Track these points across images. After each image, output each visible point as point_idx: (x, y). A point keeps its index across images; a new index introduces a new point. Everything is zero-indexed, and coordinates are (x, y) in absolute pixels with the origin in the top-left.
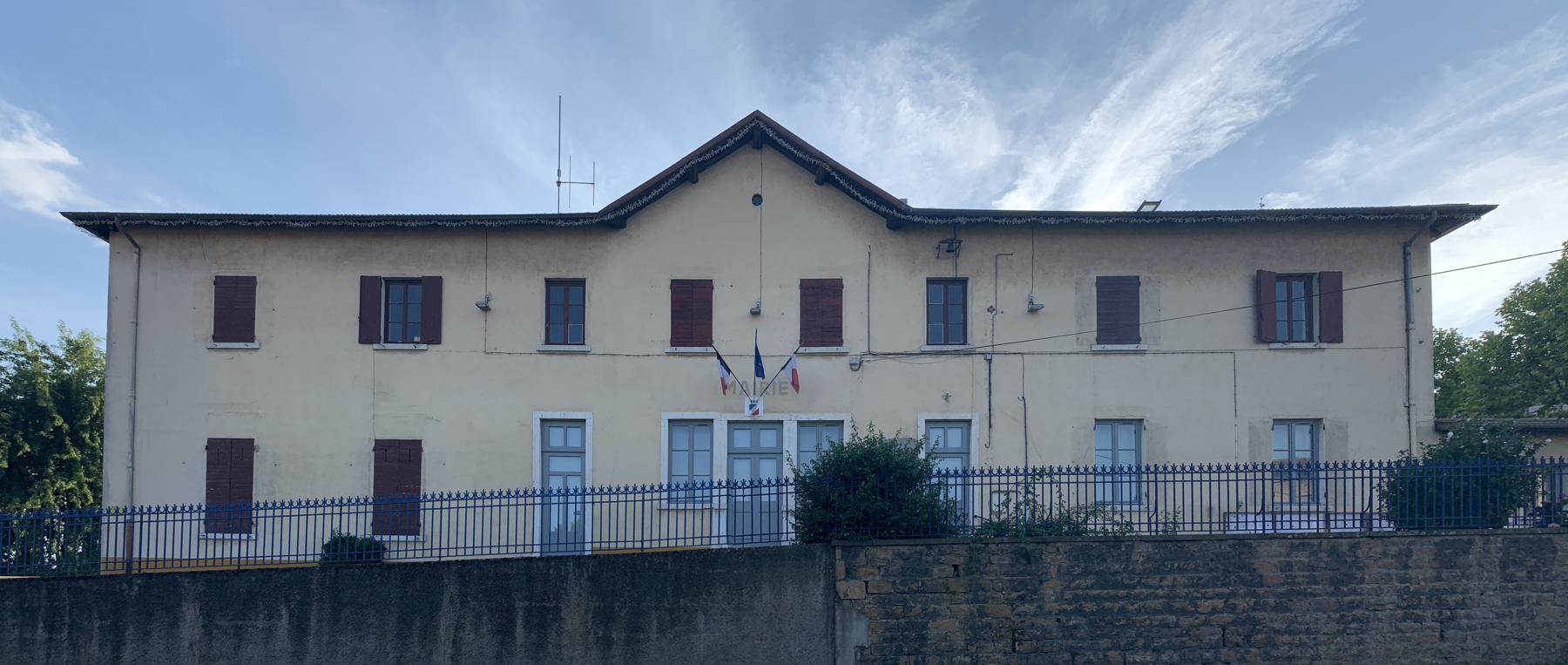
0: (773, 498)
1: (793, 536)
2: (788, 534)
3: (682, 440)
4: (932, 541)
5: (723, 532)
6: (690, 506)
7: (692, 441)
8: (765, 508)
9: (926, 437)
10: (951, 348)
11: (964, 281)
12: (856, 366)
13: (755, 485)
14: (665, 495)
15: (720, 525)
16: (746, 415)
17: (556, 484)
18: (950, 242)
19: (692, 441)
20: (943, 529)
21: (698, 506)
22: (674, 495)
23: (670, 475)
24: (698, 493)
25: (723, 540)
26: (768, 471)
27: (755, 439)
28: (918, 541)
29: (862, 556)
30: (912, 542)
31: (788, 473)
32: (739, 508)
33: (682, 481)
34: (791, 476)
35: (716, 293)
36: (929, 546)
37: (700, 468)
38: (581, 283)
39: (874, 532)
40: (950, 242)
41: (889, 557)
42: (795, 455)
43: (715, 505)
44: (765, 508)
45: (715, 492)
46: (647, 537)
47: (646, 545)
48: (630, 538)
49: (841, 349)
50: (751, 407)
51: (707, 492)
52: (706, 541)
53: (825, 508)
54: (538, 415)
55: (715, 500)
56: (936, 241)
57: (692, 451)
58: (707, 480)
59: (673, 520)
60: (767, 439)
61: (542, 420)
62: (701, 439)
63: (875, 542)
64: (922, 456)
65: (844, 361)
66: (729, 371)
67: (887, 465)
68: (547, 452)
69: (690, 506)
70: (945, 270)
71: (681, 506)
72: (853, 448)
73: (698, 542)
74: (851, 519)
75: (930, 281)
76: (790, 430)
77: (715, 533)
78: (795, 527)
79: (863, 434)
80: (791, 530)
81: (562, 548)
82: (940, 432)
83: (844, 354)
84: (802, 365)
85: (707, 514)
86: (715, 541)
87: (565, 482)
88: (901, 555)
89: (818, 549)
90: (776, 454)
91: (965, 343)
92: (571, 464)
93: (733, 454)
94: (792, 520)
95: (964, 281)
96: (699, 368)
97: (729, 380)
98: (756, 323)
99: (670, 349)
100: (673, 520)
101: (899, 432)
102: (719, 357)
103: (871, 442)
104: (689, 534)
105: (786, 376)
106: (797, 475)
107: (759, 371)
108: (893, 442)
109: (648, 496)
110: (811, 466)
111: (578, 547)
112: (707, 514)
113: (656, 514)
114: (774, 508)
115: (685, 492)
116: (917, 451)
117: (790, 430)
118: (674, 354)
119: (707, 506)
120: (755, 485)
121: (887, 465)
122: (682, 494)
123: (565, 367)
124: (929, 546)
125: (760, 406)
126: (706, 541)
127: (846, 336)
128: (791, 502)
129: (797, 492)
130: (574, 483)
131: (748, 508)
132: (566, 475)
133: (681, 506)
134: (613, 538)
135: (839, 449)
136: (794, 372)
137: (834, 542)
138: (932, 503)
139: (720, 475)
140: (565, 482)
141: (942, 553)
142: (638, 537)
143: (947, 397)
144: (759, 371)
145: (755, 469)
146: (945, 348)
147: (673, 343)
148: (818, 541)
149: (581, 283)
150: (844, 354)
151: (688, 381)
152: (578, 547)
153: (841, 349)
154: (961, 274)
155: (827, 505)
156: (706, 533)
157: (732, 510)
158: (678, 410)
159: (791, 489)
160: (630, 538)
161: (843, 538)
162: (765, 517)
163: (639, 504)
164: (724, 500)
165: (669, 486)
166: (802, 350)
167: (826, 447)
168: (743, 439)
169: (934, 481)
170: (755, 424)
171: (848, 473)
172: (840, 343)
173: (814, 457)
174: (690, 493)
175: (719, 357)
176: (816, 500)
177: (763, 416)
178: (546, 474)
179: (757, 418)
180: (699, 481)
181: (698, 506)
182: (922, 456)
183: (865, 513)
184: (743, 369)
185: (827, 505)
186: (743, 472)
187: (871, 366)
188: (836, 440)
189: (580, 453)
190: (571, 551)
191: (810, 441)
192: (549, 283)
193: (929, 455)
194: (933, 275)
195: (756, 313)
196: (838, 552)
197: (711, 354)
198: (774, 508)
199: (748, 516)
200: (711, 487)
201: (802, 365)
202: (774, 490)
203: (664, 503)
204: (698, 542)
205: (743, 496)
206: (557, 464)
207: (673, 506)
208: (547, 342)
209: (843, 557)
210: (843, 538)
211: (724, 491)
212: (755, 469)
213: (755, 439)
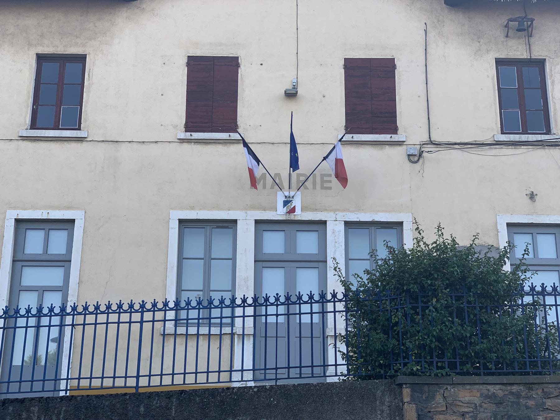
0: (316, 318)
1: (343, 369)
2: (337, 367)
3: (196, 244)
4: (532, 379)
5: (248, 364)
6: (204, 330)
7: (208, 248)
8: (306, 332)
9: (511, 245)
10: (532, 138)
11: (541, 63)
12: (415, 158)
13: (291, 301)
14: (171, 315)
15: (245, 356)
16: (280, 213)
17: (28, 301)
18: (521, 20)
19: (208, 248)
20: (545, 363)
21: (215, 330)
22: (183, 314)
23: (179, 290)
24: (216, 313)
25: (248, 376)
26: (307, 282)
27: (291, 244)
28: (512, 379)
29: (439, 398)
30: (505, 379)
31: (334, 285)
32: (271, 332)
33: (194, 298)
34: (340, 291)
35: (242, 71)
36: (530, 386)
37: (219, 282)
38: (81, 59)
39: (452, 366)
40: (521, 20)
41: (477, 401)
42: (343, 265)
43: (238, 329)
44: (306, 332)
45: (239, 311)
46: (144, 371)
47: (143, 382)
48: (120, 372)
49: (395, 138)
50: (286, 203)
51: (227, 312)
52: (224, 377)
53: (386, 332)
54: (13, 215)
55: (238, 322)
56: (504, 20)
57: (208, 259)
58: (227, 296)
59: (180, 349)
60: (307, 243)
61: (18, 221)
62: (221, 247)
63: (456, 379)
64: (507, 268)
65: (399, 153)
66: (258, 161)
67: (464, 278)
68: (20, 261)
69: (204, 330)
70: (517, 50)
71: (193, 330)
72: (418, 257)
73: (213, 377)
74: (422, 347)
75: (499, 62)
76: (336, 233)
77: (237, 366)
78: (346, 356)
79: (430, 238)
80: (340, 361)
81: (26, 387)
82: (528, 238)
83: (400, 143)
84: (351, 157)
85: (226, 341)
86: (236, 376)
87: (41, 299)
88: (492, 397)
89: (379, 386)
90: (319, 262)
91: (548, 132)
92: (50, 276)
93: (262, 261)
94: (343, 347)
95: (541, 63)
96: (219, 158)
97: (259, 172)
98: (292, 106)
99: (183, 135)
100: (180, 349)
101: (476, 237)
102: (246, 145)
103: (441, 248)
104: (202, 367)
105: (329, 166)
106: (348, 289)
107: (294, 163)
108: (470, 250)
109: (148, 316)
110: (365, 277)
111: (49, 385)
112: (226, 341)
113: (158, 339)
114: (317, 332)
115: (201, 311)
116: (500, 261)
117: (336, 233)
118: (189, 141)
119: (227, 330)
120: (291, 301)
121: (464, 278)
122: (193, 314)
123: (56, 156)
124: (530, 386)
125: (297, 203)
126: (224, 377)
127: (400, 122)
128: (338, 323)
129: (347, 310)
130: (53, 300)
131: (282, 332)
132: (42, 291)
133: (193, 330)
134: (97, 373)
135: (399, 256)
136: (339, 163)
137: (401, 379)
138: (527, 329)
139: (245, 289)
140: (41, 299)
141: (547, 396)
142: (132, 372)
143: (532, 196)
144: (294, 163)
145: (290, 281)
146: (524, 138)
147: (188, 128)
148: (378, 376)
149: (81, 59)
150: (400, 143)
151: (207, 174)
152: (49, 385)
153: (395, 138)
154: (537, 54)
155: (388, 329)
156: (225, 366)
157: (261, 336)
158: (192, 208)
159: (340, 306)
160: (120, 372)
161: (412, 374)
162: (306, 343)
163: (136, 327)
164: (250, 322)
165: (177, 303)
166: (348, 137)
167: (383, 253)
168: (275, 243)
169: (528, 299)
170: (290, 225)
171: (414, 288)
172: (394, 130)
173: (367, 265)
174: (204, 313)
175: (246, 145)
176: (373, 322)
177: (300, 215)
178: (15, 288)
179: (292, 217)
180: (216, 297)
181: (215, 330)
182: (507, 268)
183: (439, 339)
184: (276, 160)
185: (388, 329)
186: (274, 284)
187: (432, 157)
188: (394, 244)
189: (64, 262)
190: (38, 391)
191: (361, 248)
192: (41, 59)
193: (516, 267)
194: (503, 55)
195: (291, 95)
196: (406, 392)
197: (236, 142)
198: (317, 332)
199: (282, 343)
200: (233, 305)
201: (351, 157)
202: (316, 307)
203: (170, 325)
204: (213, 377)
205: (275, 315)
206: (33, 276)
207: (181, 330)
208: (33, 126)
209: (413, 399)
210: (412, 374)
211: (250, 311)
212: (290, 281)
213: (291, 244)
